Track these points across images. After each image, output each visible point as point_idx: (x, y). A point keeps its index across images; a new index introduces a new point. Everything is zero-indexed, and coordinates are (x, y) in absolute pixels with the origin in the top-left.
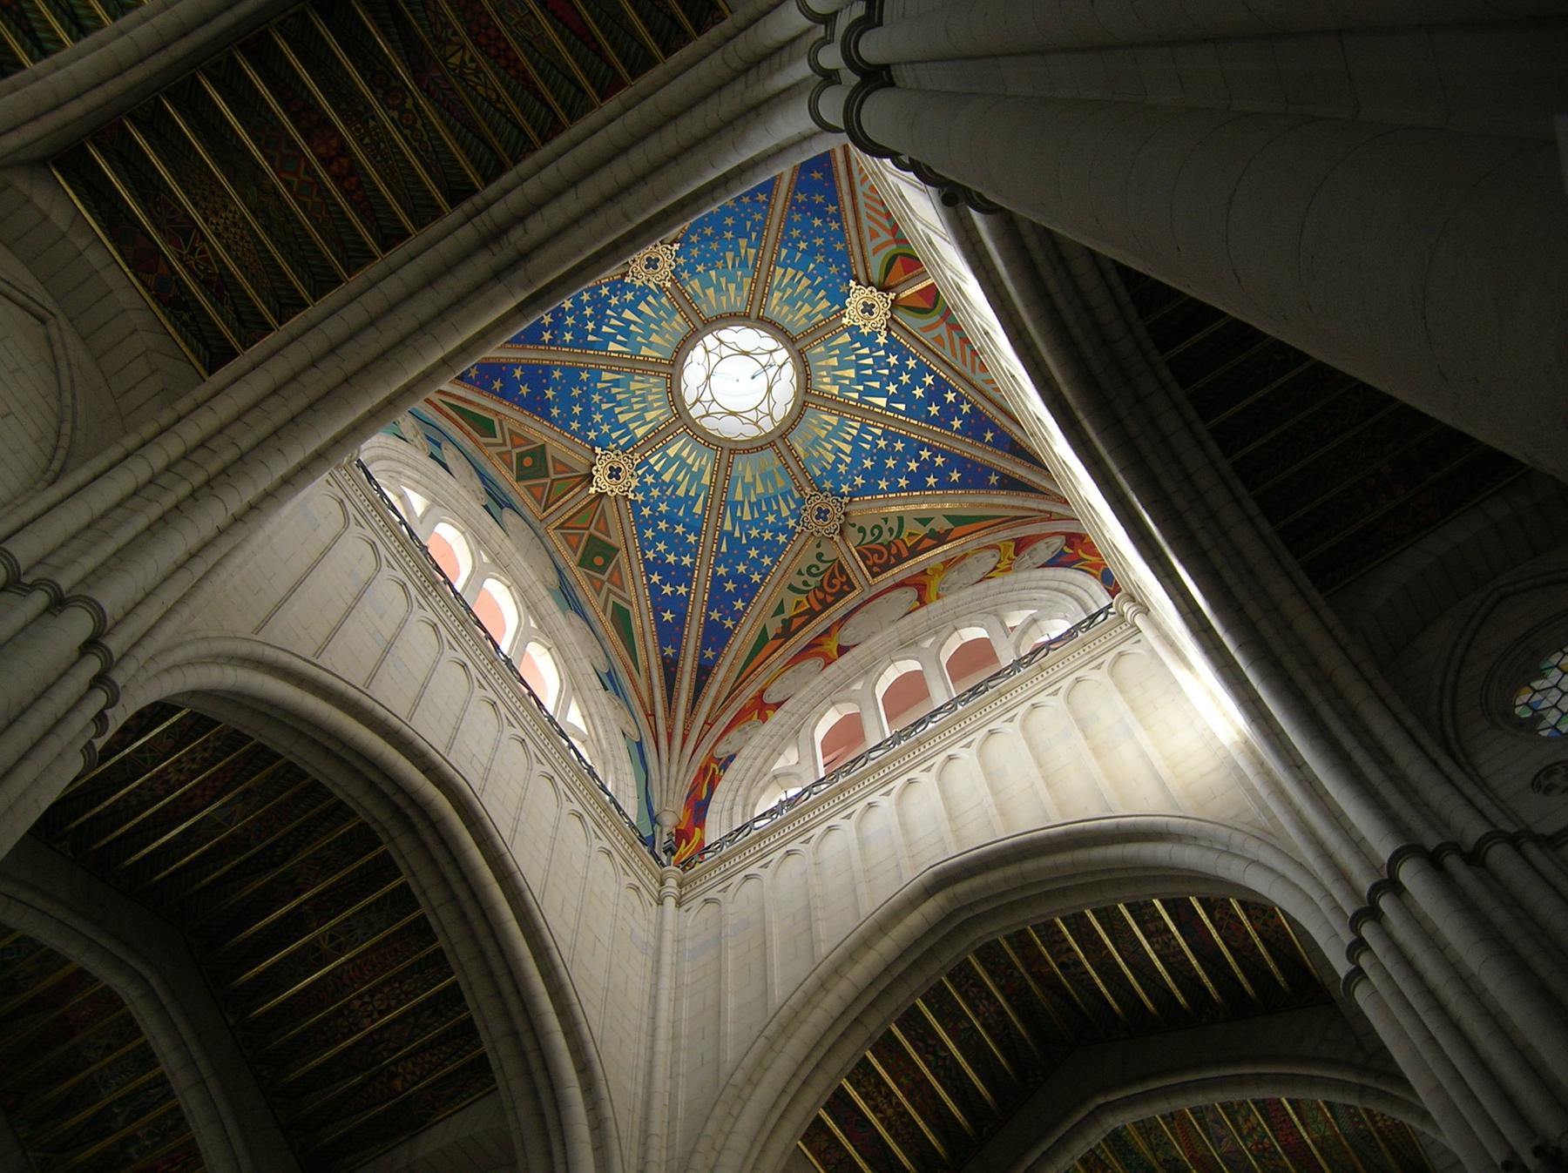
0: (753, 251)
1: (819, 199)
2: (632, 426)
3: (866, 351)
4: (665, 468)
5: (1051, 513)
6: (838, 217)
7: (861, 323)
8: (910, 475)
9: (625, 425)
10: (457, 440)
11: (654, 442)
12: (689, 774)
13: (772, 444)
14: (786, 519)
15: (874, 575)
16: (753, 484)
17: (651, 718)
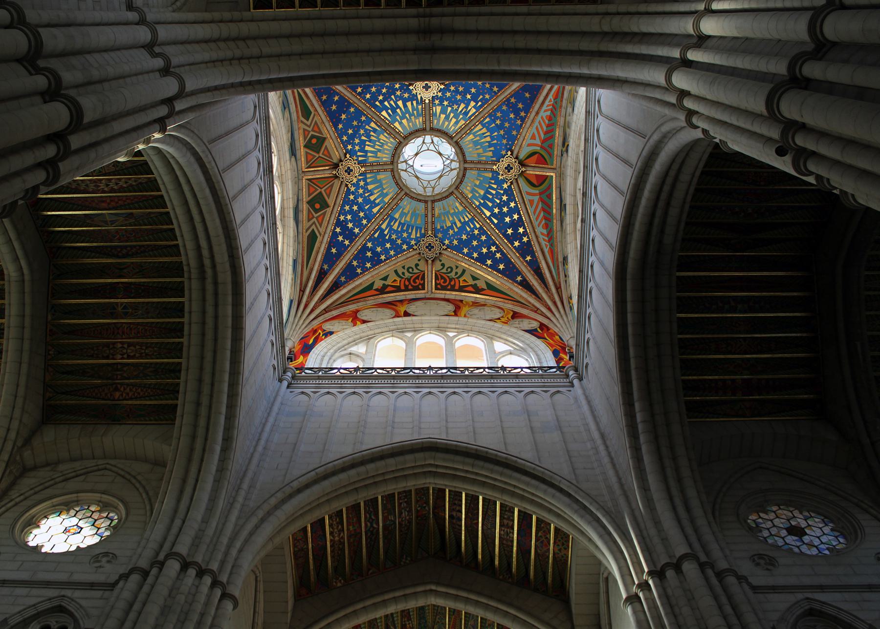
0: (474, 110)
1: (520, 106)
2: (369, 154)
3: (495, 186)
4: (371, 183)
5: (538, 309)
6: (523, 120)
7: (501, 173)
8: (480, 254)
9: (366, 152)
10: (292, 111)
11: (375, 168)
12: (307, 329)
13: (426, 202)
14: (412, 239)
15: (436, 289)
16: (406, 215)
17: (301, 293)
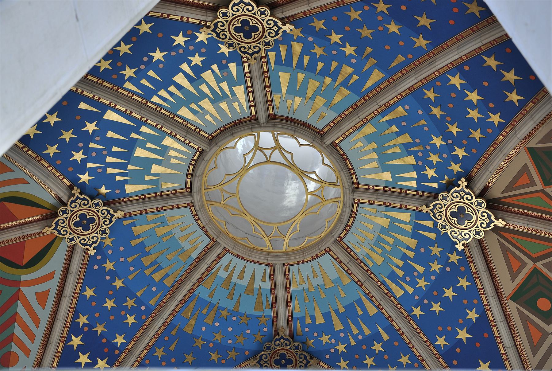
2: (409, 228)
3: (110, 171)
9: (414, 235)
16: (317, 92)
